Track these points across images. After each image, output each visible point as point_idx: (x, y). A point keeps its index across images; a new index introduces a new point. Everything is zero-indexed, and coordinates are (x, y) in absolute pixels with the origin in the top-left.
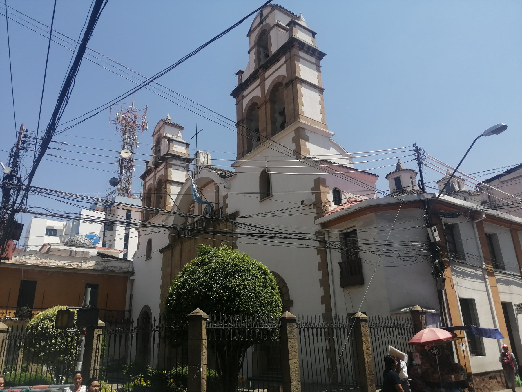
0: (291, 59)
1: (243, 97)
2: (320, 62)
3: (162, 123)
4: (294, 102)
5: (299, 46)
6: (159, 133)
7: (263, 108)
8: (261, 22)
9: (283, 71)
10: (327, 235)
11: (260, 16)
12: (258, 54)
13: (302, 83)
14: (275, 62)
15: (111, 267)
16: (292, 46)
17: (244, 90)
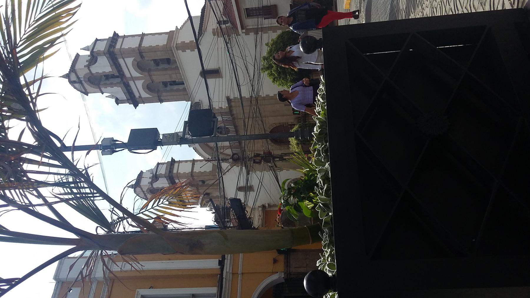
0: (122, 54)
1: (140, 97)
2: (120, 35)
3: (138, 189)
4: (156, 52)
5: (112, 48)
6: (145, 192)
7: (154, 78)
8: (80, 82)
9: (130, 61)
10: (248, 27)
11: (74, 83)
12: (106, 86)
13: (141, 46)
14: (120, 67)
15: (259, 222)
16: (113, 52)
17: (134, 96)
